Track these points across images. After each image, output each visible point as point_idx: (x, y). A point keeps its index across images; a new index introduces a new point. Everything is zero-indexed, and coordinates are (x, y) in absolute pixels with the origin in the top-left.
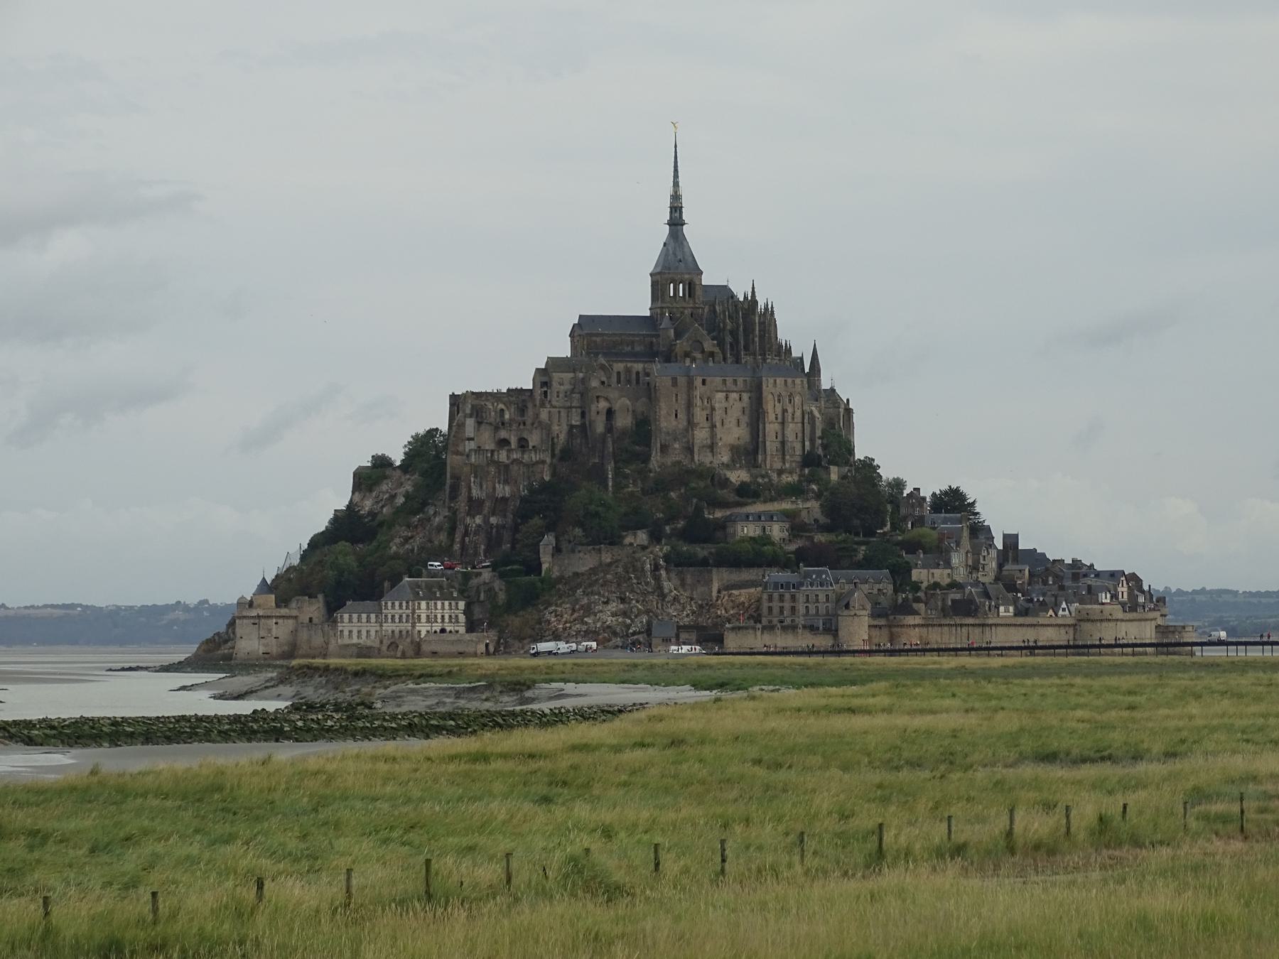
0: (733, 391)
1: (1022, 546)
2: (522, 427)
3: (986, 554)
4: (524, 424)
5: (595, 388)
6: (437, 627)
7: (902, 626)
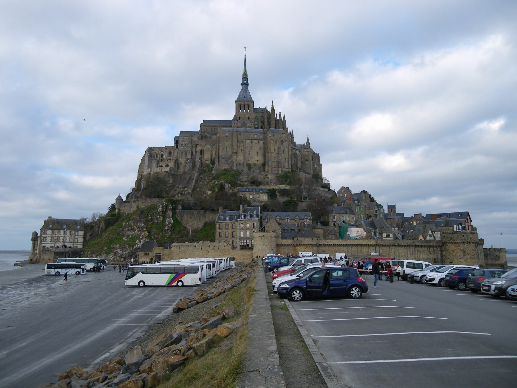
0: (254, 140)
1: (398, 211)
2: (169, 159)
3: (377, 209)
4: (170, 159)
6: (60, 245)
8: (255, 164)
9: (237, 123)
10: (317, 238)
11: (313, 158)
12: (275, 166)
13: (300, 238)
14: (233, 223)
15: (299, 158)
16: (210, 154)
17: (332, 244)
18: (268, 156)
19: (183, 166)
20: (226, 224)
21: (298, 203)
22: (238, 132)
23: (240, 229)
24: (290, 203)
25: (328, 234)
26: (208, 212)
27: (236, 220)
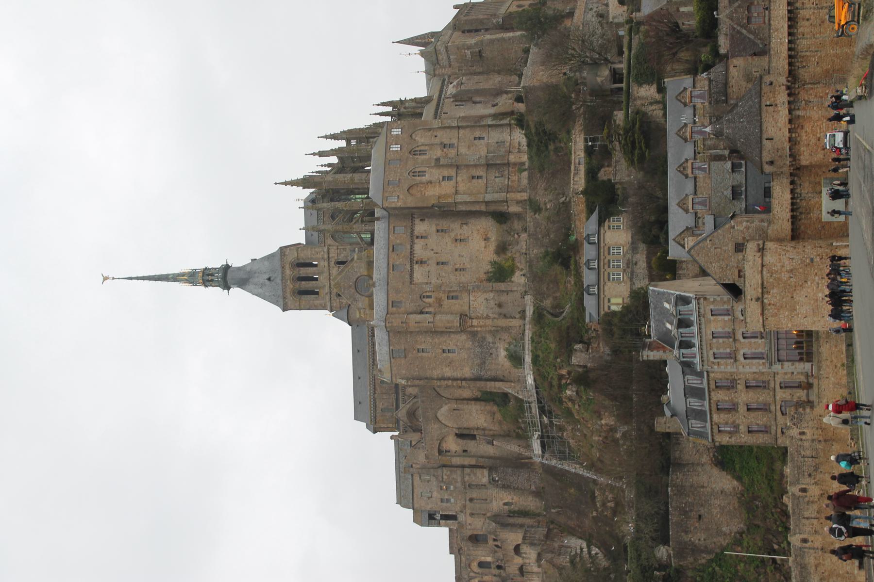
0: (412, 253)
2: (496, 543)
4: (495, 540)
5: (427, 457)
7: (793, 142)
8: (502, 249)
9: (359, 309)
10: (765, 88)
11: (469, 31)
12: (502, 176)
13: (765, 154)
14: (713, 386)
15: (471, 84)
16: (470, 407)
17: (789, 27)
18: (466, 203)
19: (516, 499)
20: (718, 409)
21: (638, 112)
22: (387, 314)
23: (736, 360)
24: (633, 143)
25: (750, 32)
26: (677, 454)
27: (700, 375)
